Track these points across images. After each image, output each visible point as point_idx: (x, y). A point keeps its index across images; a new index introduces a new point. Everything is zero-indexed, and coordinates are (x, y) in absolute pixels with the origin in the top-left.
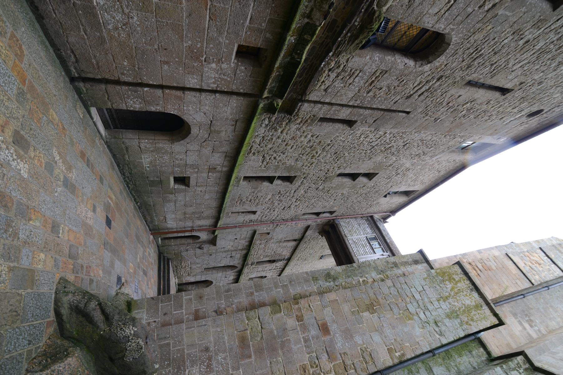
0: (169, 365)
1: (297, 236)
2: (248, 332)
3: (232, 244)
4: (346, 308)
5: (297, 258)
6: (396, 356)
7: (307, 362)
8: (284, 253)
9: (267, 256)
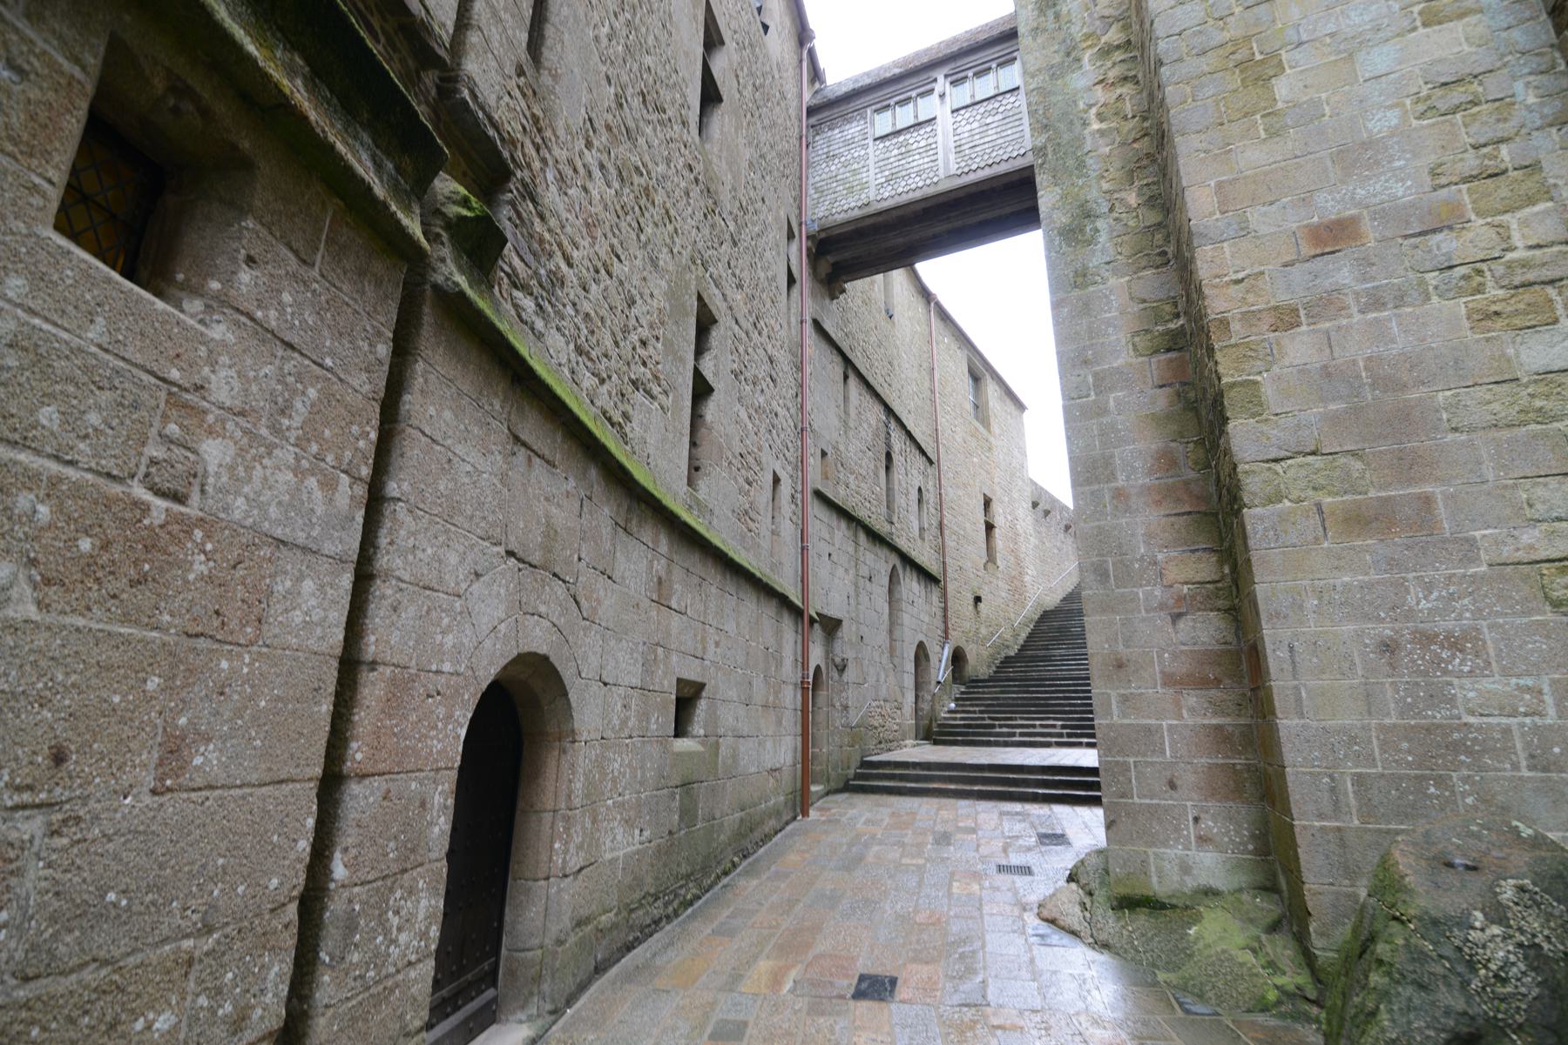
0: (1440, 781)
1: (837, 369)
2: (1329, 500)
3: (840, 572)
4: (1253, 156)
5: (886, 385)
7: (1460, 306)
8: (873, 422)
9: (876, 475)
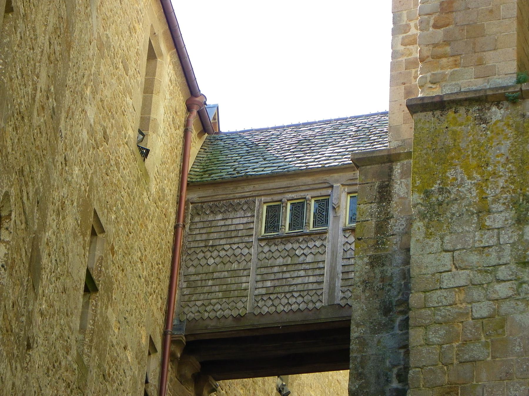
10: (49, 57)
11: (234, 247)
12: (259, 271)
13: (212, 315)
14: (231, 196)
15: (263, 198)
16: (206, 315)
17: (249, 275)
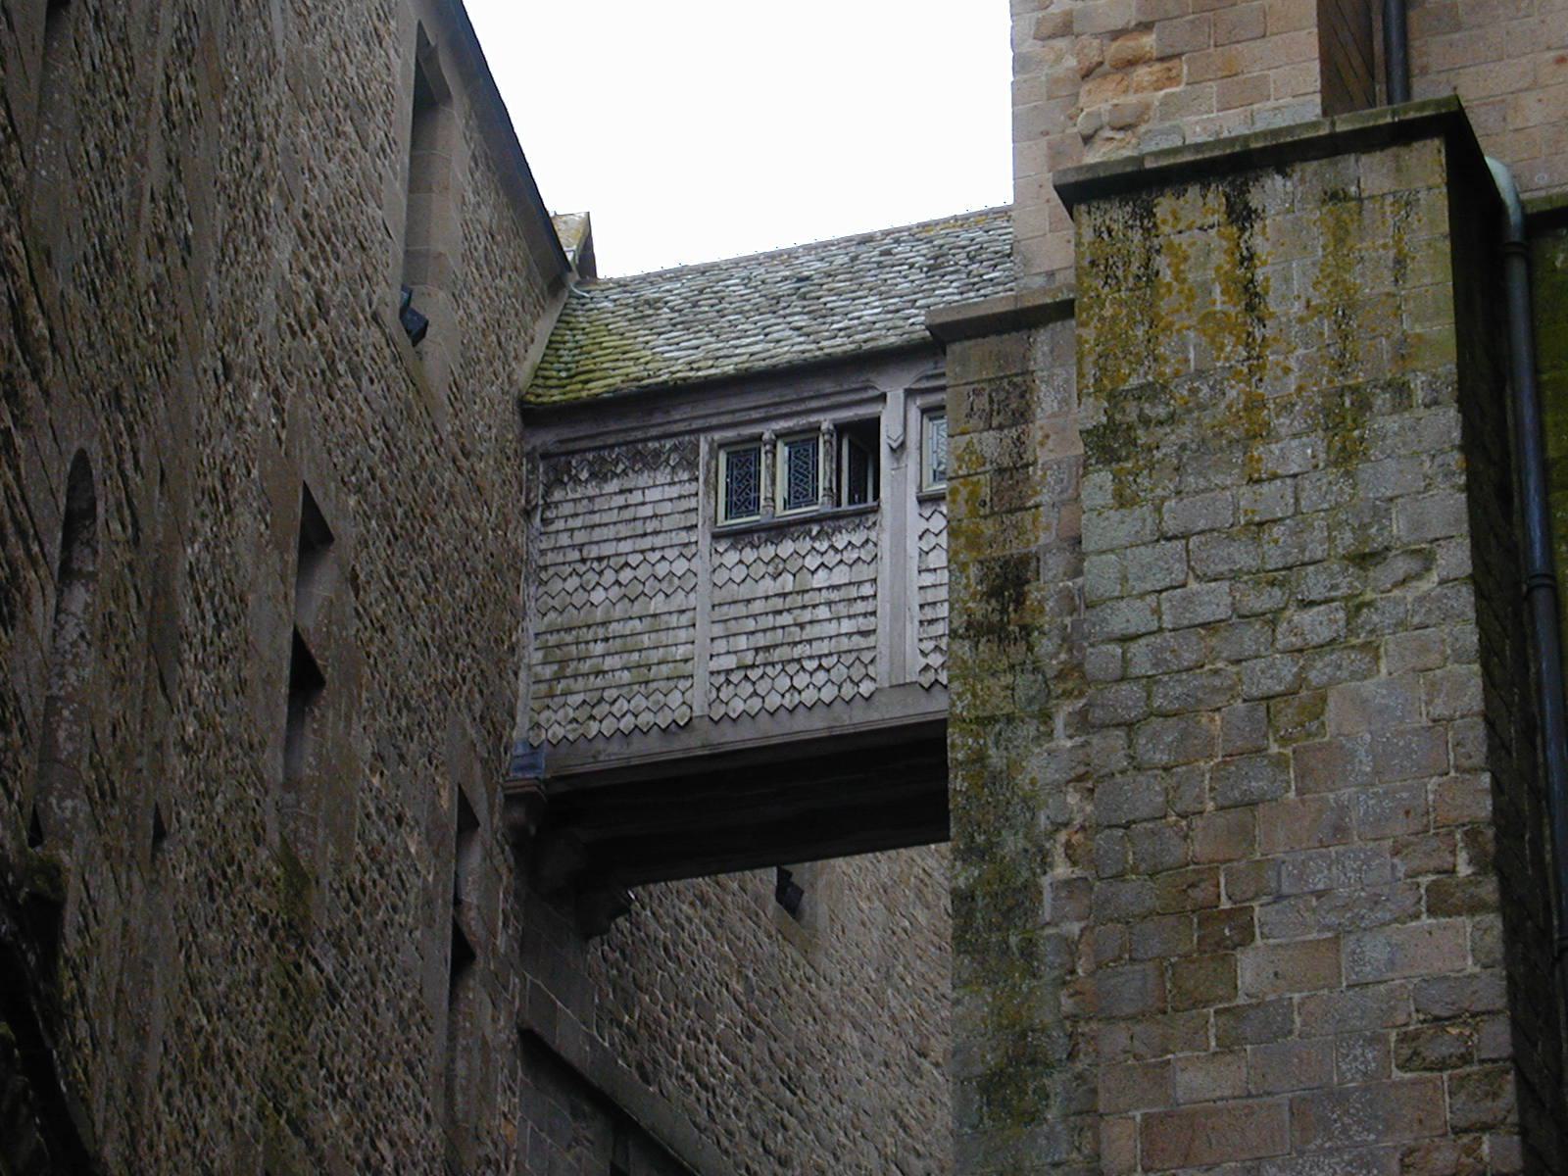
6: (1469, 881)
10: (168, 113)
11: (654, 557)
12: (718, 614)
13: (608, 727)
14: (640, 435)
15: (717, 436)
16: (594, 727)
17: (694, 625)
